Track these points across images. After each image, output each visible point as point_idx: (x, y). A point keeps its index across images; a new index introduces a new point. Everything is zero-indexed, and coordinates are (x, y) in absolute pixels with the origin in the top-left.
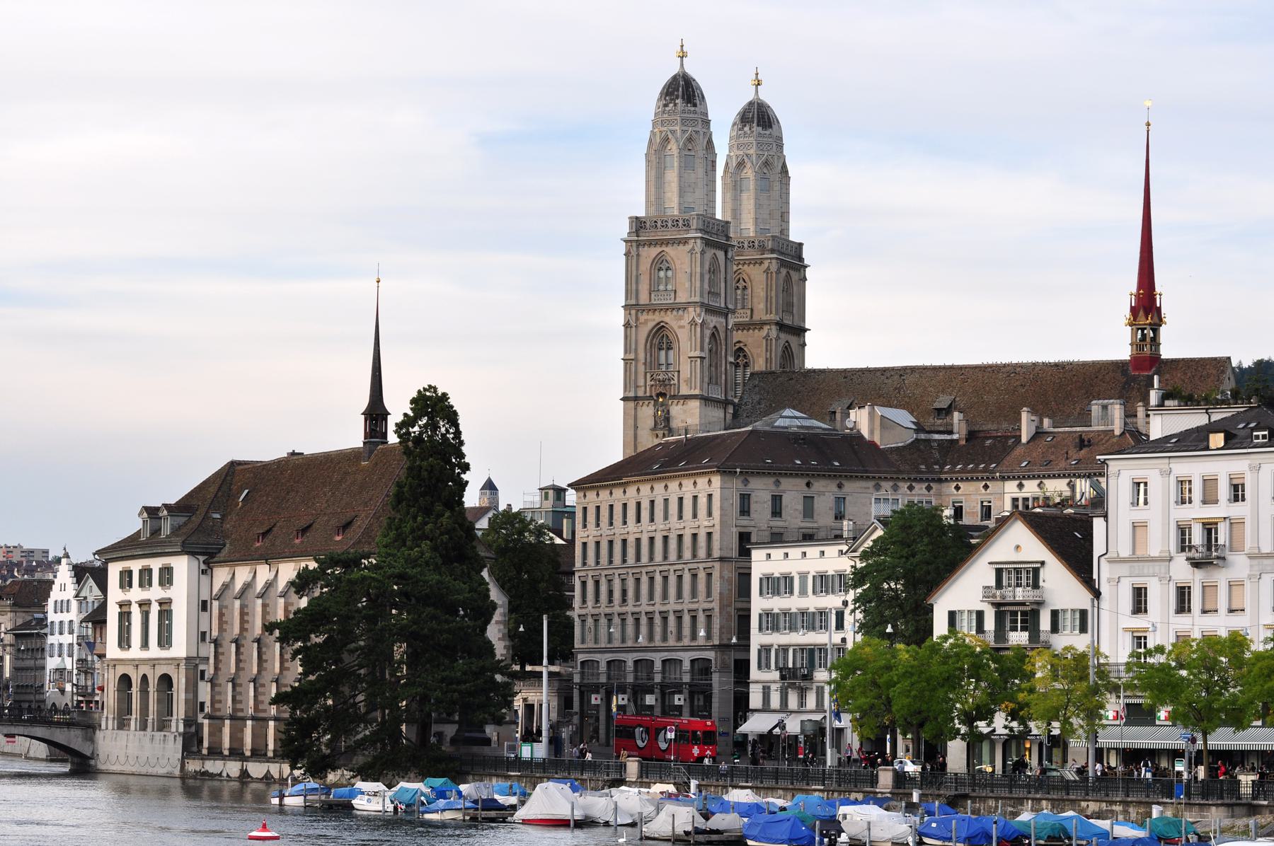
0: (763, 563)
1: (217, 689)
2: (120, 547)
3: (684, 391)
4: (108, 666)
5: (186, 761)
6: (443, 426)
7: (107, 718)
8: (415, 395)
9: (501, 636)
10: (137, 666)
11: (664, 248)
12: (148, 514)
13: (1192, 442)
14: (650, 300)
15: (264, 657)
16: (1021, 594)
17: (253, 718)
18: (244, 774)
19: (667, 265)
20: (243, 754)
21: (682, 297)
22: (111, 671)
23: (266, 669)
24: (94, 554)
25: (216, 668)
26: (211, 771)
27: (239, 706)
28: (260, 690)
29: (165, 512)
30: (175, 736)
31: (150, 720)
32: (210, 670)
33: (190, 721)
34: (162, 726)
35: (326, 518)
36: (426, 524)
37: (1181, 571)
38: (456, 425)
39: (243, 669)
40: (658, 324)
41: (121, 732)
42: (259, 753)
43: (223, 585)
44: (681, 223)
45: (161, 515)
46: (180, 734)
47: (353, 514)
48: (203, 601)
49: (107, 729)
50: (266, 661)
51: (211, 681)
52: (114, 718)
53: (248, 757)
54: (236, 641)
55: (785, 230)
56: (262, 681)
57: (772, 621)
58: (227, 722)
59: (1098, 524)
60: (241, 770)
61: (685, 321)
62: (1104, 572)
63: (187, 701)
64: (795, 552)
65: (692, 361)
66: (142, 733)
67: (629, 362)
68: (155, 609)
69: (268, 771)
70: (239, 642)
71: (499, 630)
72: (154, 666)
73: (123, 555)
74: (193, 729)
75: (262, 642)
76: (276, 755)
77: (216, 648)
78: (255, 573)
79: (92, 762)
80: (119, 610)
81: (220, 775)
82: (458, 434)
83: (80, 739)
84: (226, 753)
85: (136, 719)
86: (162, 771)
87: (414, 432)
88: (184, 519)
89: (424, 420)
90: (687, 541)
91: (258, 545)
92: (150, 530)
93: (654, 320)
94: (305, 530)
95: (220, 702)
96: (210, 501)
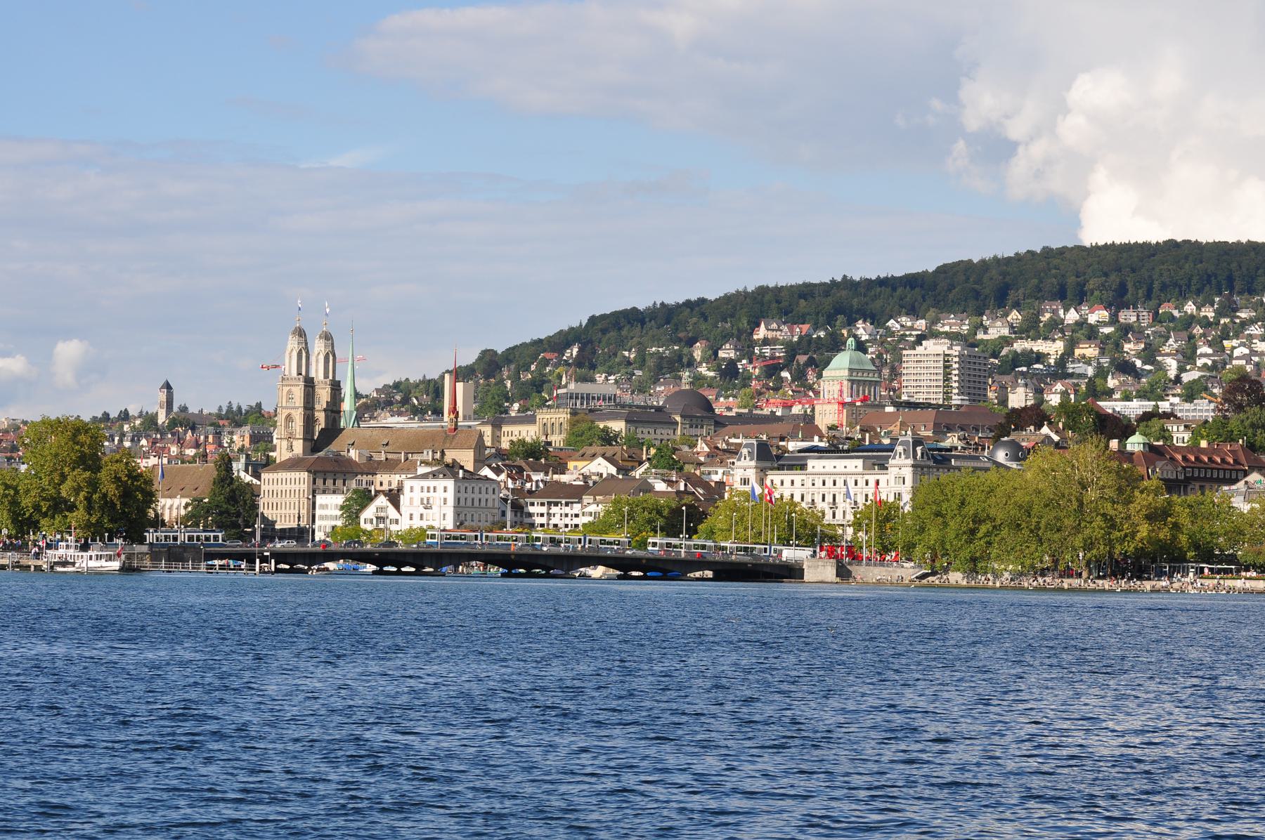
0: (320, 499)
3: (298, 436)
13: (424, 476)
16: (382, 514)
21: (297, 405)
37: (422, 510)
55: (334, 377)
57: (322, 518)
59: (401, 496)
61: (298, 413)
62: (402, 509)
64: (329, 496)
90: (297, 491)
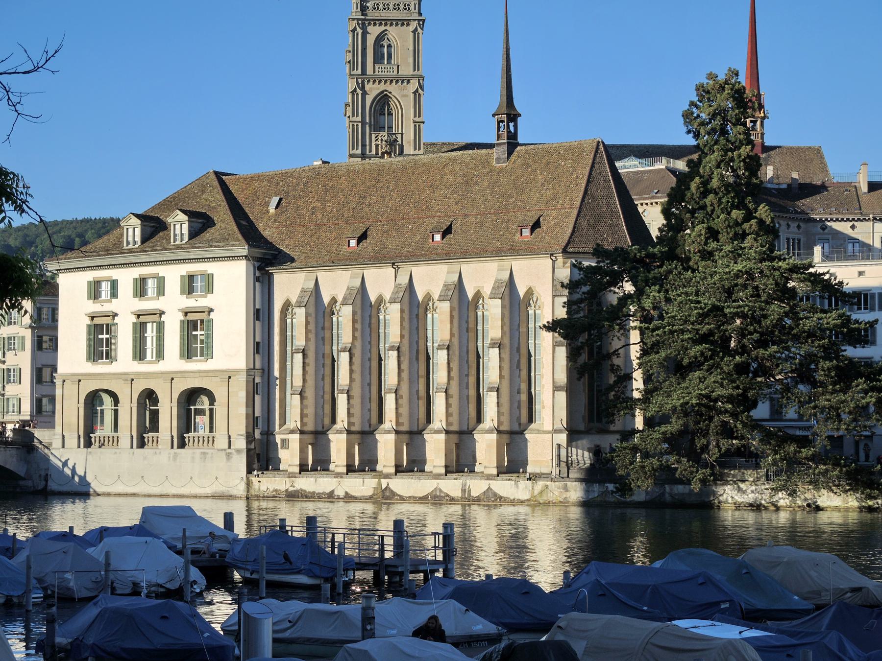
1: (305, 402)
11: (388, 27)
14: (374, 72)
19: (389, 42)
40: (383, 92)
44: (402, 7)
65: (415, 126)
67: (355, 124)
70: (352, 352)
75: (400, 350)
83: (14, 459)
86: (209, 491)
93: (379, 89)
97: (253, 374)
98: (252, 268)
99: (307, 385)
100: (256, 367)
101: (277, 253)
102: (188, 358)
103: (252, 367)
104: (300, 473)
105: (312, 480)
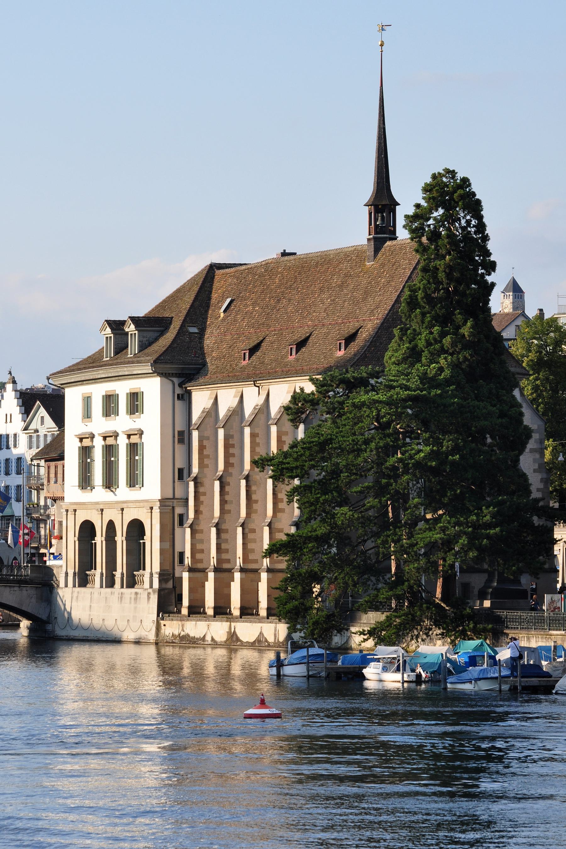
1: (198, 536)
2: (80, 369)
4: (67, 511)
5: (162, 622)
6: (464, 217)
7: (67, 574)
8: (429, 180)
9: (536, 466)
10: (102, 510)
12: (112, 329)
15: (254, 497)
17: (242, 570)
18: (233, 637)
20: (230, 613)
22: (71, 517)
23: (256, 511)
24: (48, 379)
25: (197, 512)
26: (192, 635)
27: (224, 556)
28: (250, 536)
29: (132, 327)
30: (149, 593)
31: (118, 574)
32: (191, 515)
33: (166, 575)
34: (131, 582)
35: (325, 330)
36: (443, 335)
38: (480, 218)
39: (229, 512)
41: (83, 589)
42: (250, 611)
43: (203, 412)
45: (127, 330)
46: (154, 591)
47: (357, 325)
48: (179, 432)
49: (66, 586)
50: (256, 502)
51: (191, 526)
52: (75, 573)
53: (237, 618)
54: (220, 479)
56: (251, 526)
58: (211, 575)
60: (229, 633)
63: (162, 552)
66: (109, 590)
68: (122, 442)
69: (261, 633)
70: (224, 480)
71: (535, 461)
72: (122, 510)
73: (83, 379)
74: (170, 585)
75: (250, 479)
76: (270, 613)
77: (196, 487)
78: (242, 396)
79: (49, 627)
80: (79, 444)
81: (203, 639)
82: (481, 227)
83: (34, 600)
84: (210, 612)
85: (102, 574)
87: (429, 226)
88: (151, 335)
89: (441, 211)
91: (244, 363)
92: (115, 348)
94: (301, 344)
95: (202, 551)
96: (185, 312)
97: (171, 504)
98: (169, 386)
99: (201, 517)
100: (176, 496)
101: (201, 366)
102: (130, 487)
103: (171, 496)
104: (189, 616)
105: (194, 622)
